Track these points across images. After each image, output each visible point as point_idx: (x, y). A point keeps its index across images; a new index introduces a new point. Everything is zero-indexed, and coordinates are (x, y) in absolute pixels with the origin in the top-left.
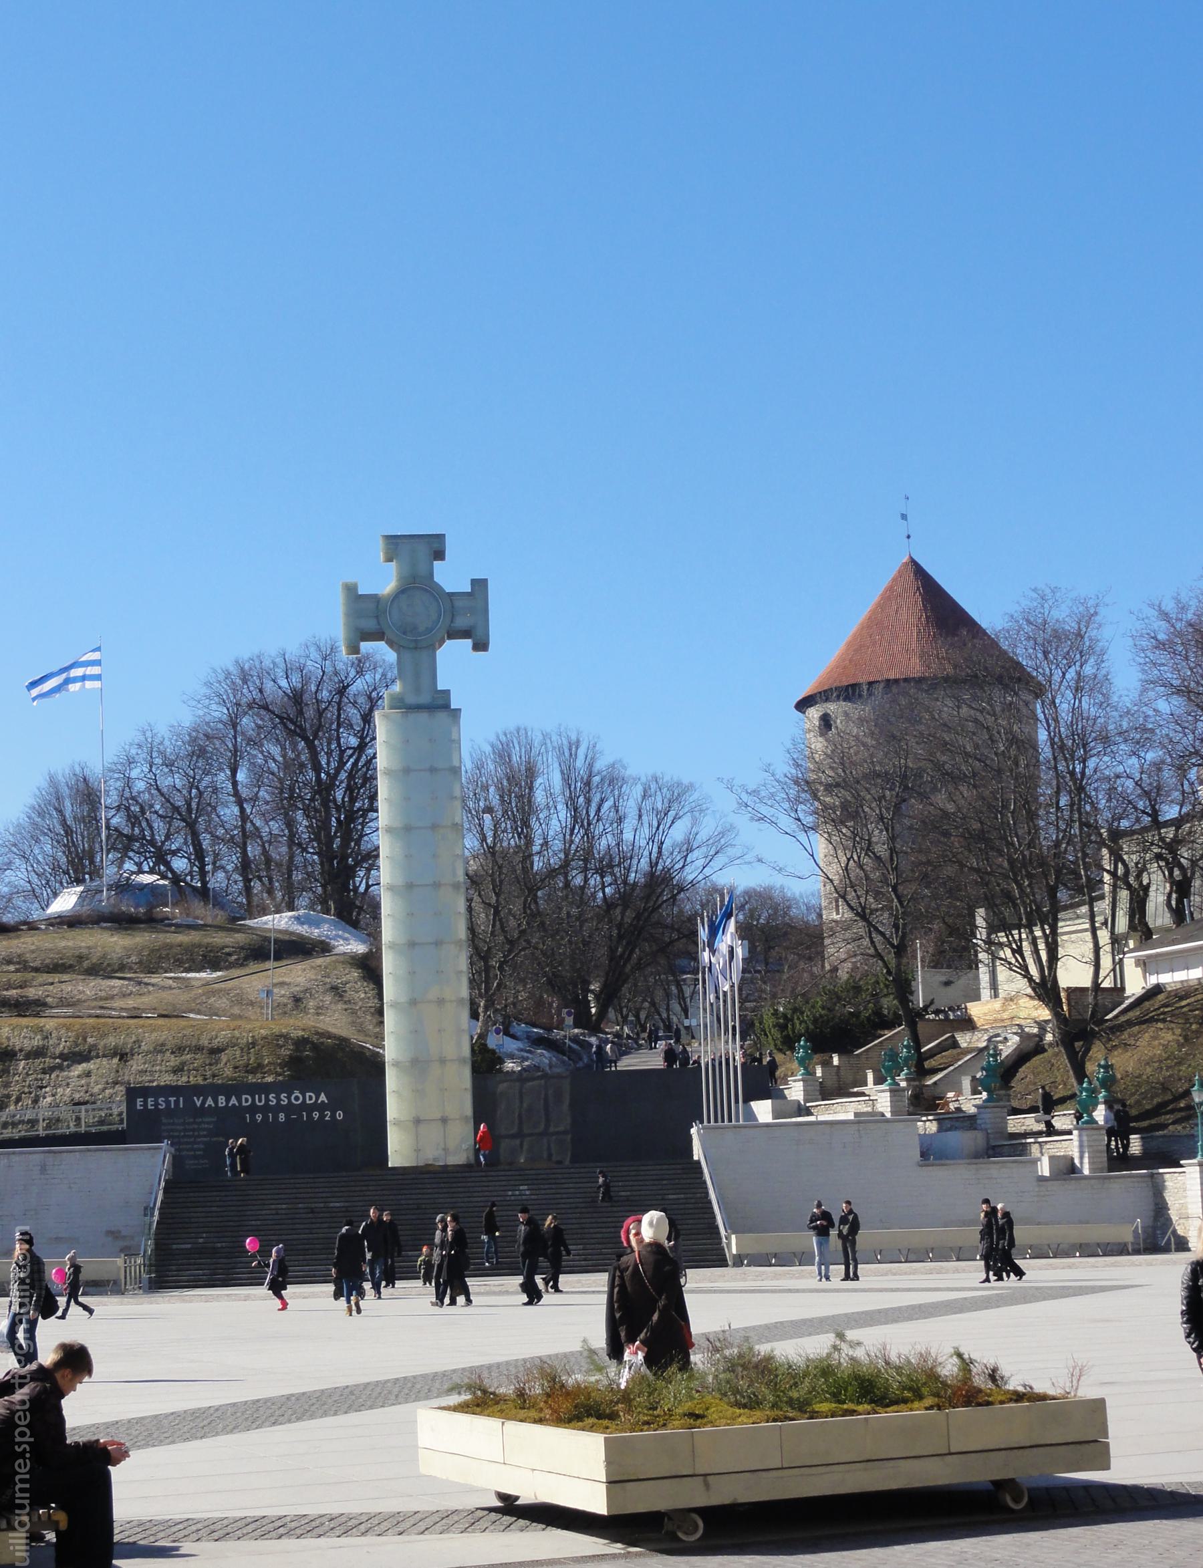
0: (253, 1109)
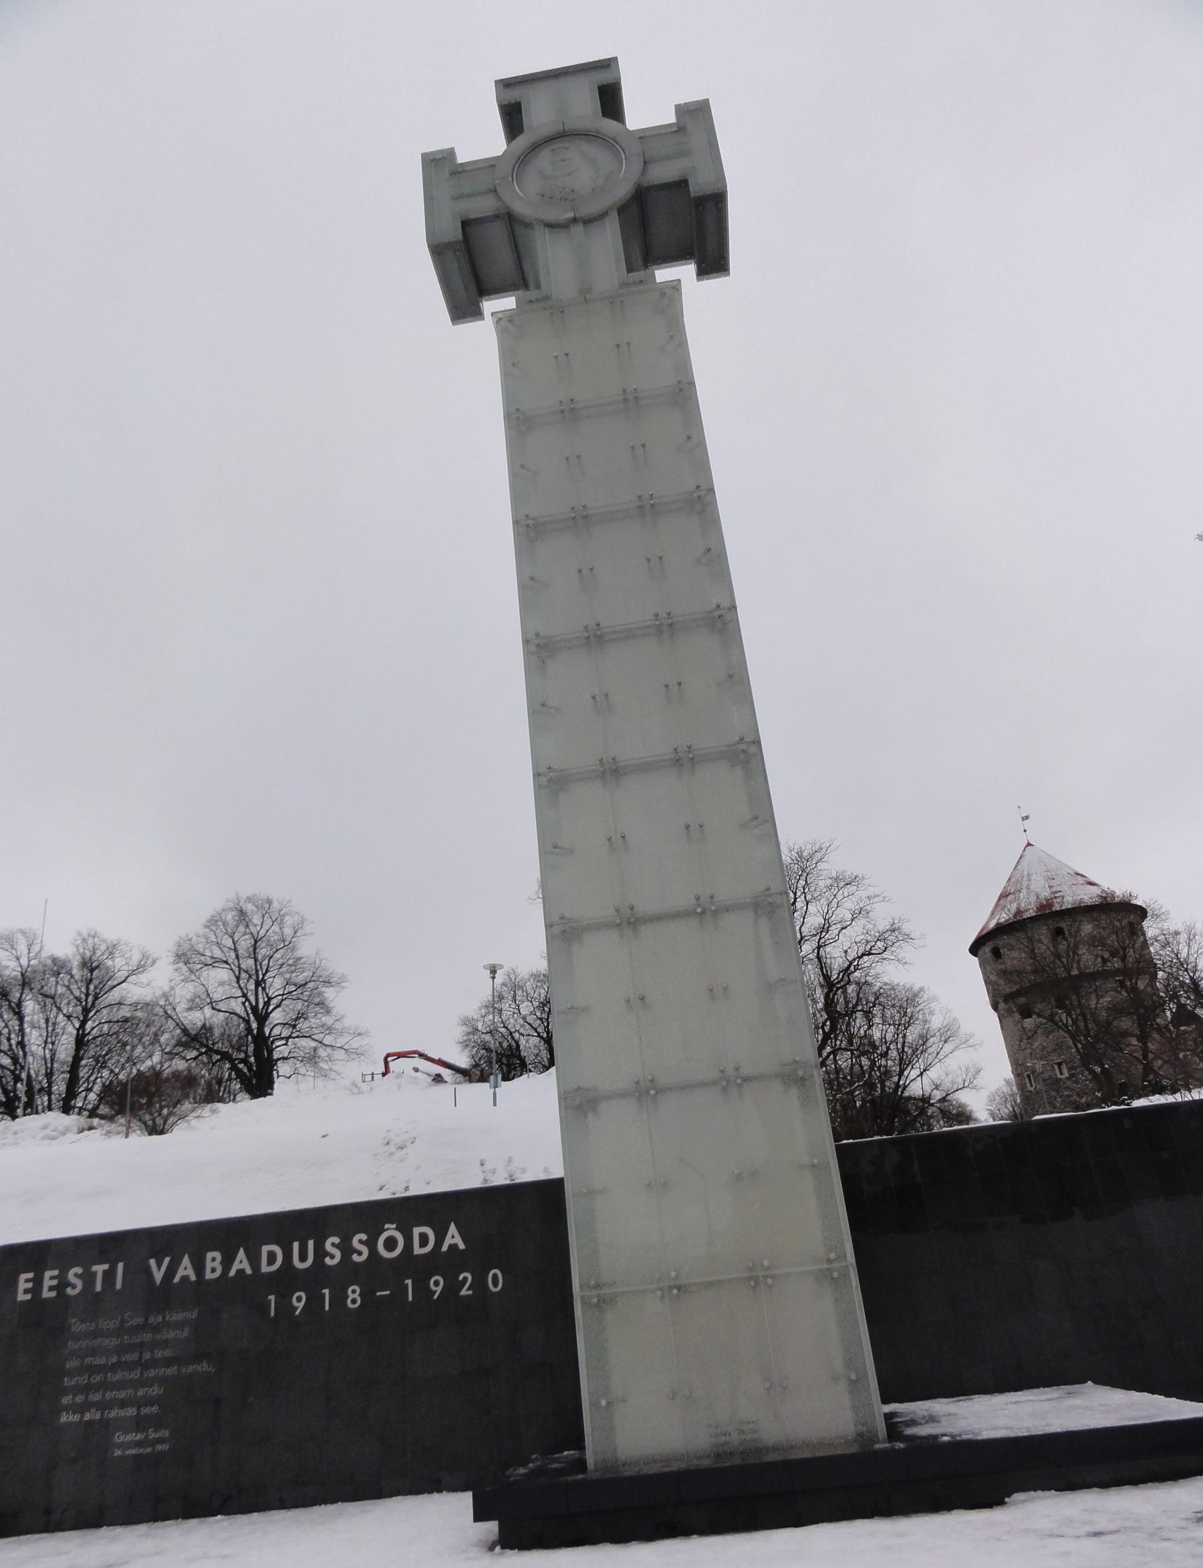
0: (286, 1279)
